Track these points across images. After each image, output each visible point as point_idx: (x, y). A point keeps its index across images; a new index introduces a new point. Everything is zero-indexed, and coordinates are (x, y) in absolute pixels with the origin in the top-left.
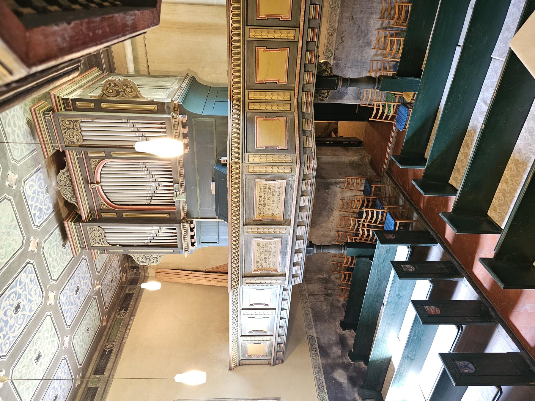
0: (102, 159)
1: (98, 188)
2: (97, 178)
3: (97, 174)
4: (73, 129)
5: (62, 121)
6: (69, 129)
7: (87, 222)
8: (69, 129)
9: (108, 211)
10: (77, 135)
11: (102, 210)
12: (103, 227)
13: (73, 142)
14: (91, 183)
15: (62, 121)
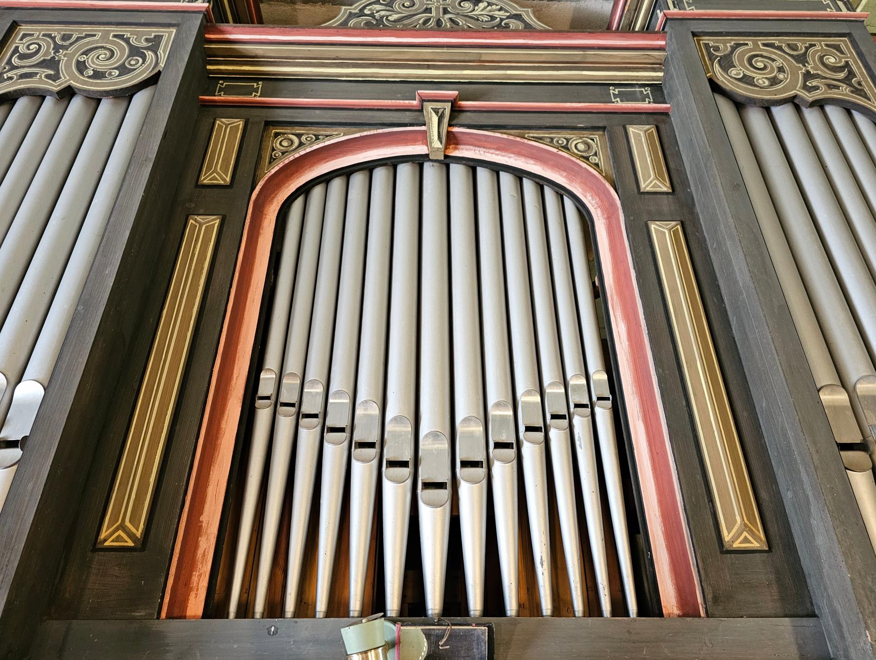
0: (622, 176)
1: (424, 137)
2: (478, 143)
3: (502, 147)
4: (808, 76)
5: (837, 48)
6: (802, 59)
7: (201, 39)
8: (802, 59)
9: (250, 157)
10: (774, 81)
11: (263, 126)
12: (140, 99)
13: (726, 63)
14: (456, 110)
15: (837, 48)
